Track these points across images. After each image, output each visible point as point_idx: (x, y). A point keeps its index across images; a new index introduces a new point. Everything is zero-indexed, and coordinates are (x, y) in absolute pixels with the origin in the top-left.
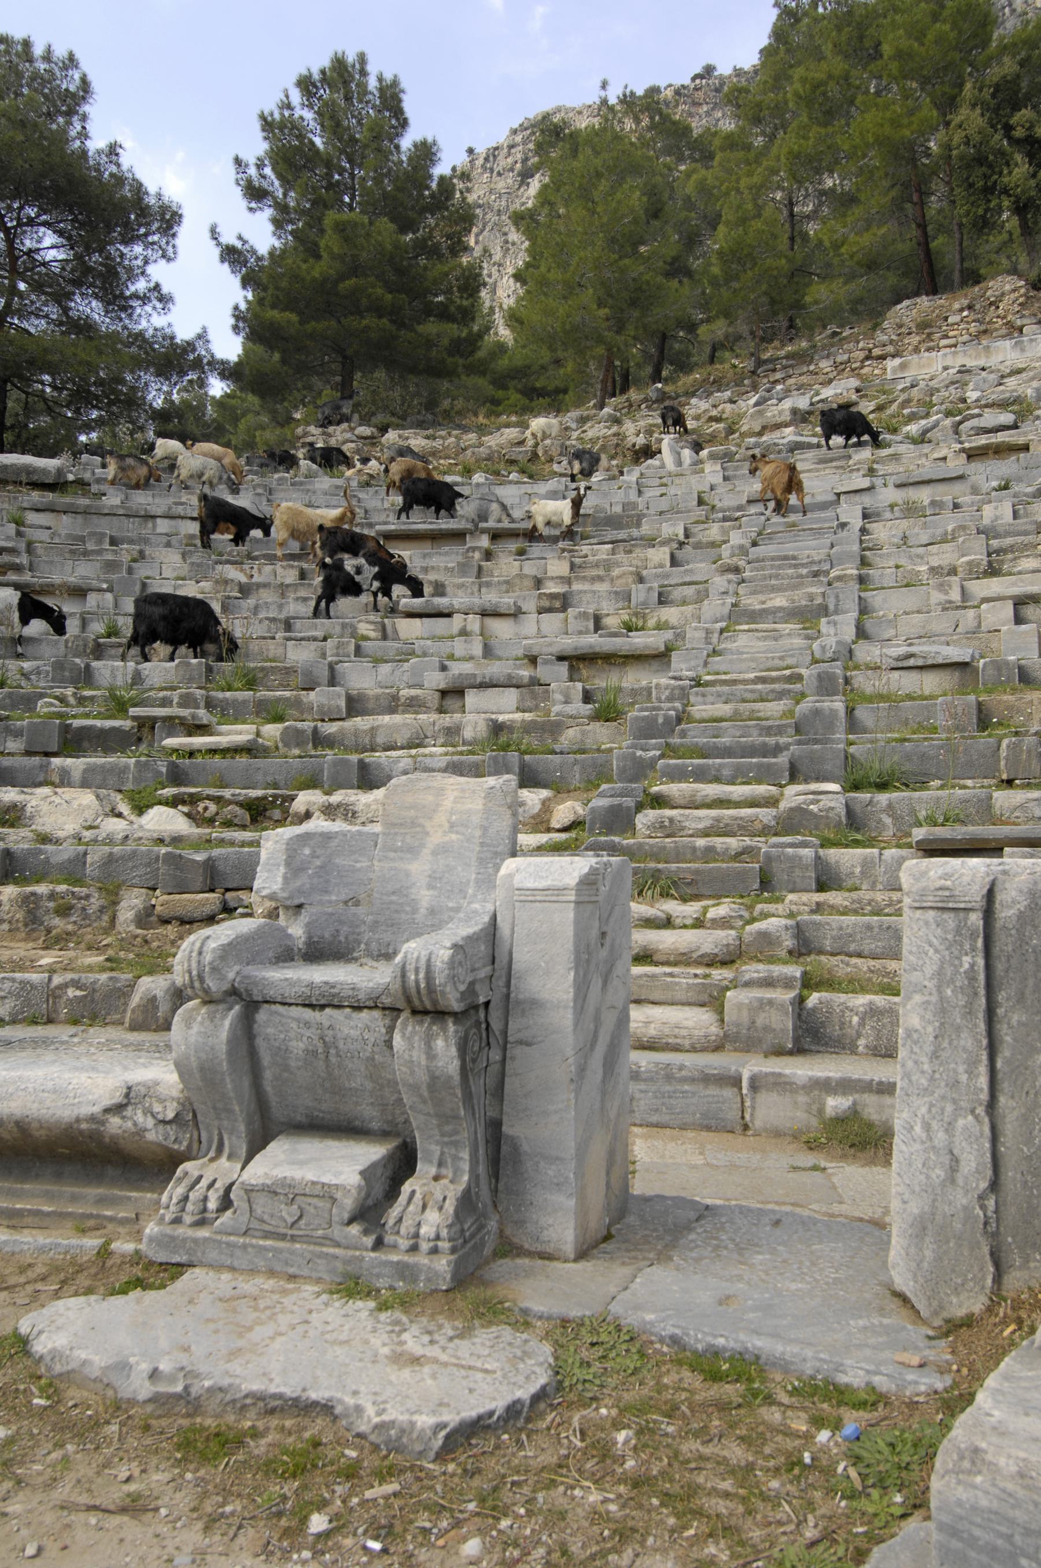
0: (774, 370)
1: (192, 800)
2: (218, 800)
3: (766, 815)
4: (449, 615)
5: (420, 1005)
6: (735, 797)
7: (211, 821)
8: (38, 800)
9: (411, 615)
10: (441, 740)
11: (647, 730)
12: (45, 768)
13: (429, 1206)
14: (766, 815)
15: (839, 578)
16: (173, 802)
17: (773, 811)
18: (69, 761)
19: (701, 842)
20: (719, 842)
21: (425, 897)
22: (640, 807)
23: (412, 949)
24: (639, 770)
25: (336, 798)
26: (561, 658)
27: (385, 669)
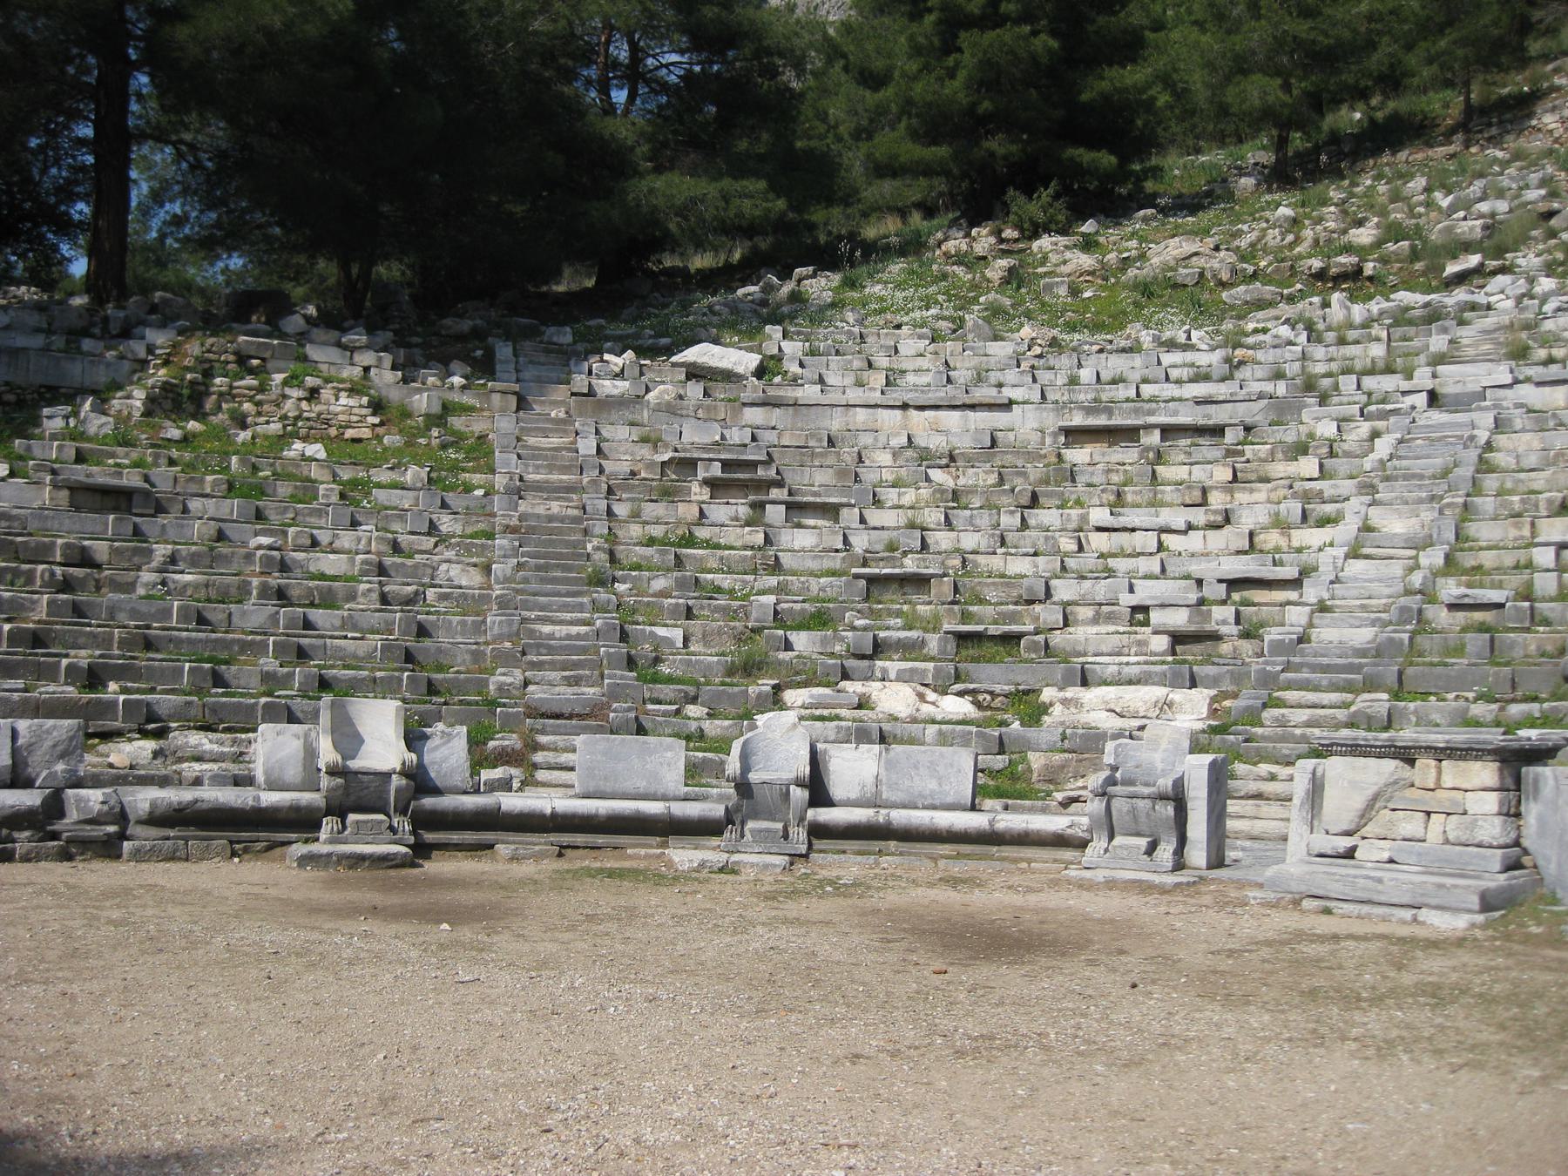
0: (1490, 125)
1: (973, 692)
2: (991, 693)
3: (1341, 714)
4: (1133, 530)
5: (1163, 797)
6: (1325, 702)
7: (989, 708)
8: (874, 689)
9: (1099, 529)
10: (1133, 651)
11: (1278, 648)
12: (872, 668)
13: (1166, 852)
14: (1341, 714)
15: (1449, 505)
16: (960, 694)
17: (1345, 712)
18: (888, 663)
19: (1298, 731)
20: (1308, 731)
21: (1160, 766)
22: (1265, 706)
23: (1161, 782)
24: (1268, 680)
25: (1070, 692)
26: (1220, 581)
27: (1087, 584)
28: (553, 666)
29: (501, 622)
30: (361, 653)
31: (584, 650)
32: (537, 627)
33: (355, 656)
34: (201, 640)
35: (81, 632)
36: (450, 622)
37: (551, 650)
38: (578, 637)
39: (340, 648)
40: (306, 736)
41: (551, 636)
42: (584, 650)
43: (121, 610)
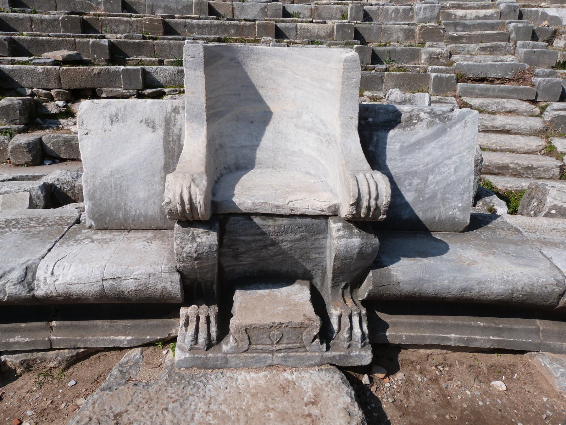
28: (471, 39)
29: (425, 8)
30: (322, 33)
31: (493, 27)
32: (452, 11)
33: (318, 36)
34: (207, 26)
35: (120, 21)
36: (387, 11)
37: (465, 27)
38: (485, 17)
39: (307, 30)
40: (168, 123)
41: (464, 17)
42: (493, 27)
43: (158, 7)
